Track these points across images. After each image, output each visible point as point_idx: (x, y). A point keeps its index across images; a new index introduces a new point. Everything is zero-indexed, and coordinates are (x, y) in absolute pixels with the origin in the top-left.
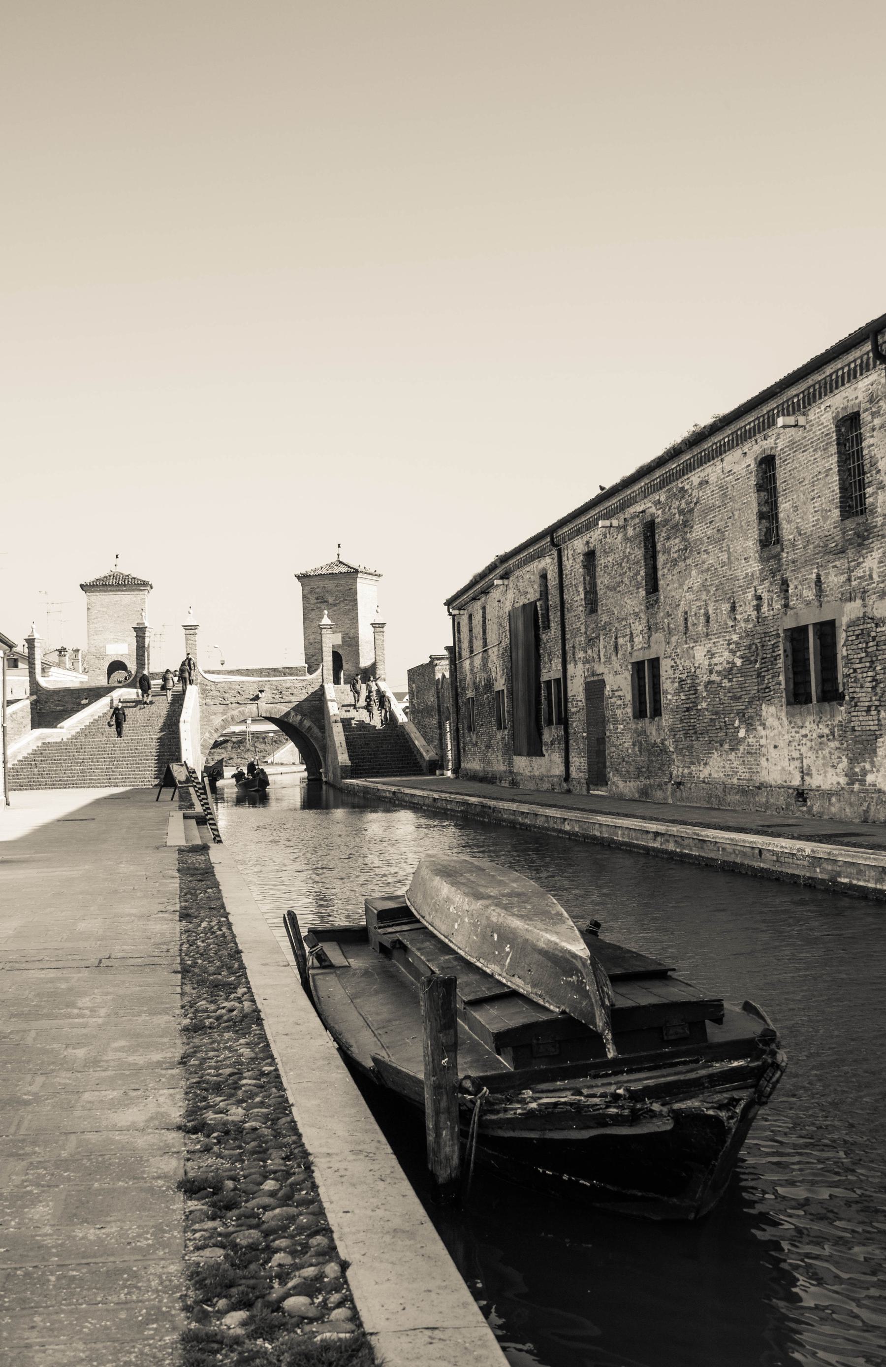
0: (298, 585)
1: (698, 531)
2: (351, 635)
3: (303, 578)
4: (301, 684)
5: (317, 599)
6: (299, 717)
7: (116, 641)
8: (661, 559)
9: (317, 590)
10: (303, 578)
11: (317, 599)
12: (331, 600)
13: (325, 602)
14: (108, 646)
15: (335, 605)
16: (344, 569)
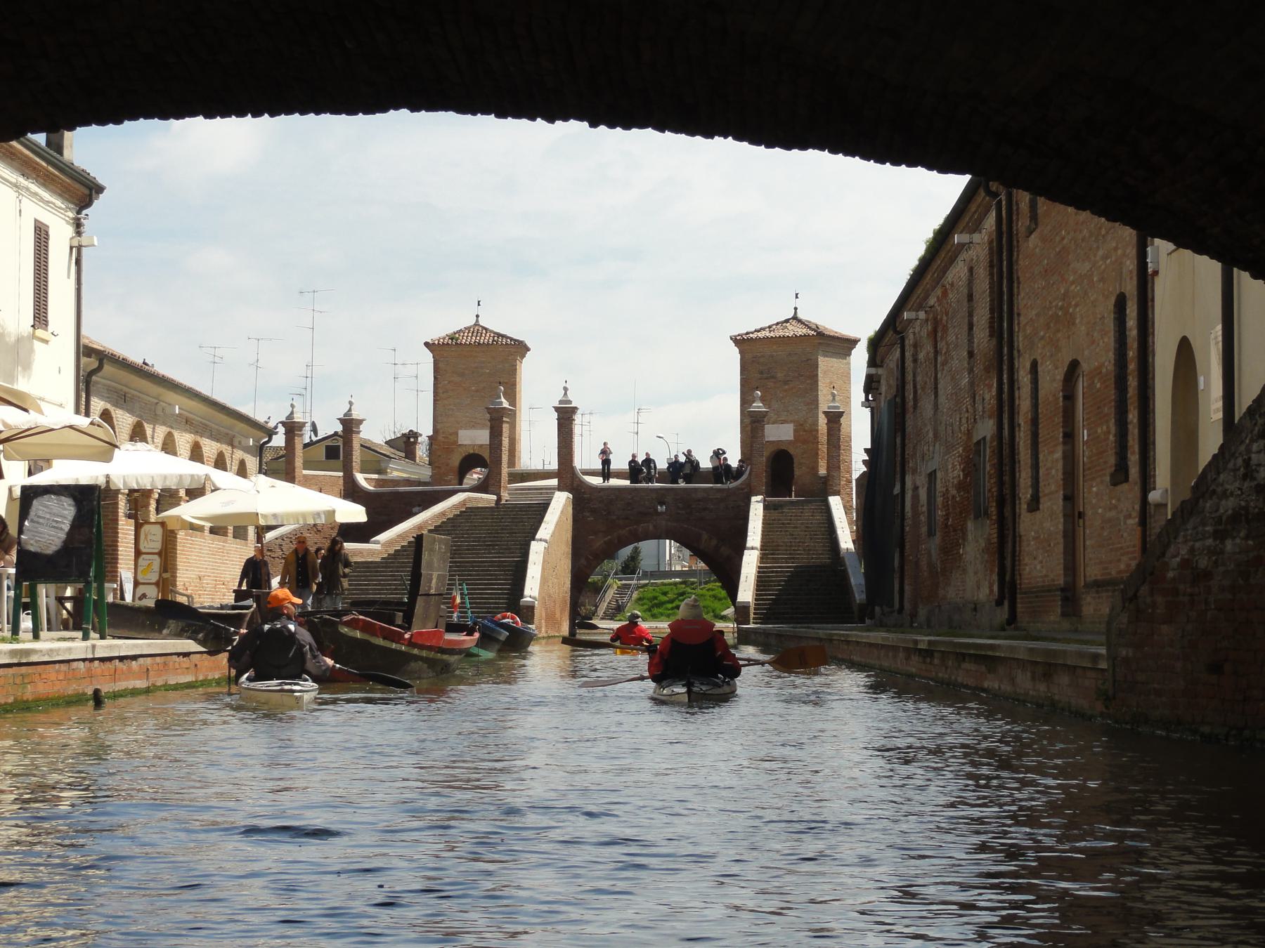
0: (734, 354)
1: (951, 338)
2: (807, 426)
3: (742, 342)
4: (718, 496)
5: (761, 373)
6: (714, 542)
7: (474, 425)
8: (939, 358)
9: (762, 360)
10: (742, 342)
11: (761, 373)
12: (780, 375)
13: (773, 377)
14: (462, 433)
15: (786, 383)
16: (801, 331)
